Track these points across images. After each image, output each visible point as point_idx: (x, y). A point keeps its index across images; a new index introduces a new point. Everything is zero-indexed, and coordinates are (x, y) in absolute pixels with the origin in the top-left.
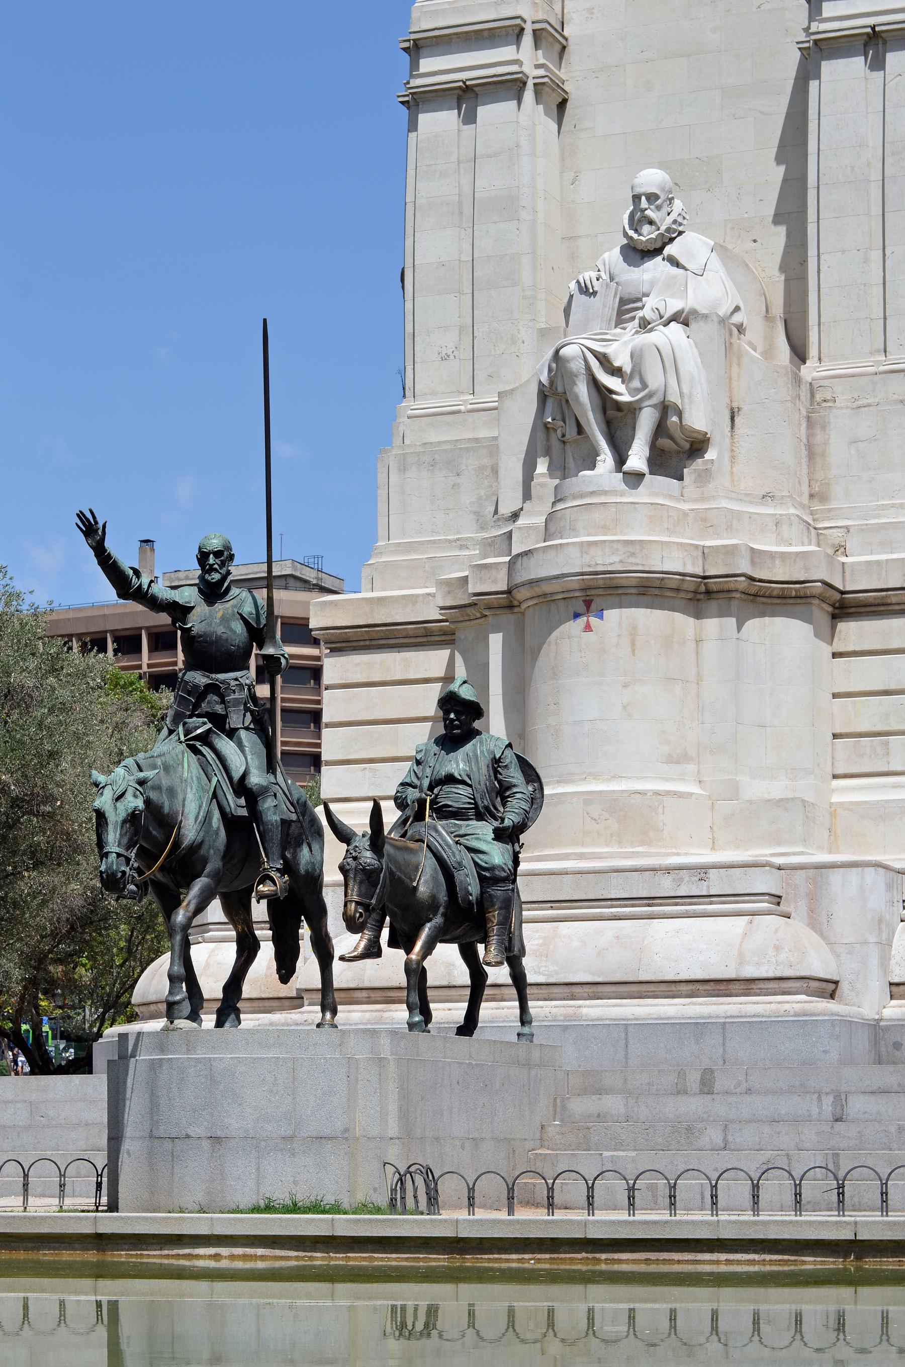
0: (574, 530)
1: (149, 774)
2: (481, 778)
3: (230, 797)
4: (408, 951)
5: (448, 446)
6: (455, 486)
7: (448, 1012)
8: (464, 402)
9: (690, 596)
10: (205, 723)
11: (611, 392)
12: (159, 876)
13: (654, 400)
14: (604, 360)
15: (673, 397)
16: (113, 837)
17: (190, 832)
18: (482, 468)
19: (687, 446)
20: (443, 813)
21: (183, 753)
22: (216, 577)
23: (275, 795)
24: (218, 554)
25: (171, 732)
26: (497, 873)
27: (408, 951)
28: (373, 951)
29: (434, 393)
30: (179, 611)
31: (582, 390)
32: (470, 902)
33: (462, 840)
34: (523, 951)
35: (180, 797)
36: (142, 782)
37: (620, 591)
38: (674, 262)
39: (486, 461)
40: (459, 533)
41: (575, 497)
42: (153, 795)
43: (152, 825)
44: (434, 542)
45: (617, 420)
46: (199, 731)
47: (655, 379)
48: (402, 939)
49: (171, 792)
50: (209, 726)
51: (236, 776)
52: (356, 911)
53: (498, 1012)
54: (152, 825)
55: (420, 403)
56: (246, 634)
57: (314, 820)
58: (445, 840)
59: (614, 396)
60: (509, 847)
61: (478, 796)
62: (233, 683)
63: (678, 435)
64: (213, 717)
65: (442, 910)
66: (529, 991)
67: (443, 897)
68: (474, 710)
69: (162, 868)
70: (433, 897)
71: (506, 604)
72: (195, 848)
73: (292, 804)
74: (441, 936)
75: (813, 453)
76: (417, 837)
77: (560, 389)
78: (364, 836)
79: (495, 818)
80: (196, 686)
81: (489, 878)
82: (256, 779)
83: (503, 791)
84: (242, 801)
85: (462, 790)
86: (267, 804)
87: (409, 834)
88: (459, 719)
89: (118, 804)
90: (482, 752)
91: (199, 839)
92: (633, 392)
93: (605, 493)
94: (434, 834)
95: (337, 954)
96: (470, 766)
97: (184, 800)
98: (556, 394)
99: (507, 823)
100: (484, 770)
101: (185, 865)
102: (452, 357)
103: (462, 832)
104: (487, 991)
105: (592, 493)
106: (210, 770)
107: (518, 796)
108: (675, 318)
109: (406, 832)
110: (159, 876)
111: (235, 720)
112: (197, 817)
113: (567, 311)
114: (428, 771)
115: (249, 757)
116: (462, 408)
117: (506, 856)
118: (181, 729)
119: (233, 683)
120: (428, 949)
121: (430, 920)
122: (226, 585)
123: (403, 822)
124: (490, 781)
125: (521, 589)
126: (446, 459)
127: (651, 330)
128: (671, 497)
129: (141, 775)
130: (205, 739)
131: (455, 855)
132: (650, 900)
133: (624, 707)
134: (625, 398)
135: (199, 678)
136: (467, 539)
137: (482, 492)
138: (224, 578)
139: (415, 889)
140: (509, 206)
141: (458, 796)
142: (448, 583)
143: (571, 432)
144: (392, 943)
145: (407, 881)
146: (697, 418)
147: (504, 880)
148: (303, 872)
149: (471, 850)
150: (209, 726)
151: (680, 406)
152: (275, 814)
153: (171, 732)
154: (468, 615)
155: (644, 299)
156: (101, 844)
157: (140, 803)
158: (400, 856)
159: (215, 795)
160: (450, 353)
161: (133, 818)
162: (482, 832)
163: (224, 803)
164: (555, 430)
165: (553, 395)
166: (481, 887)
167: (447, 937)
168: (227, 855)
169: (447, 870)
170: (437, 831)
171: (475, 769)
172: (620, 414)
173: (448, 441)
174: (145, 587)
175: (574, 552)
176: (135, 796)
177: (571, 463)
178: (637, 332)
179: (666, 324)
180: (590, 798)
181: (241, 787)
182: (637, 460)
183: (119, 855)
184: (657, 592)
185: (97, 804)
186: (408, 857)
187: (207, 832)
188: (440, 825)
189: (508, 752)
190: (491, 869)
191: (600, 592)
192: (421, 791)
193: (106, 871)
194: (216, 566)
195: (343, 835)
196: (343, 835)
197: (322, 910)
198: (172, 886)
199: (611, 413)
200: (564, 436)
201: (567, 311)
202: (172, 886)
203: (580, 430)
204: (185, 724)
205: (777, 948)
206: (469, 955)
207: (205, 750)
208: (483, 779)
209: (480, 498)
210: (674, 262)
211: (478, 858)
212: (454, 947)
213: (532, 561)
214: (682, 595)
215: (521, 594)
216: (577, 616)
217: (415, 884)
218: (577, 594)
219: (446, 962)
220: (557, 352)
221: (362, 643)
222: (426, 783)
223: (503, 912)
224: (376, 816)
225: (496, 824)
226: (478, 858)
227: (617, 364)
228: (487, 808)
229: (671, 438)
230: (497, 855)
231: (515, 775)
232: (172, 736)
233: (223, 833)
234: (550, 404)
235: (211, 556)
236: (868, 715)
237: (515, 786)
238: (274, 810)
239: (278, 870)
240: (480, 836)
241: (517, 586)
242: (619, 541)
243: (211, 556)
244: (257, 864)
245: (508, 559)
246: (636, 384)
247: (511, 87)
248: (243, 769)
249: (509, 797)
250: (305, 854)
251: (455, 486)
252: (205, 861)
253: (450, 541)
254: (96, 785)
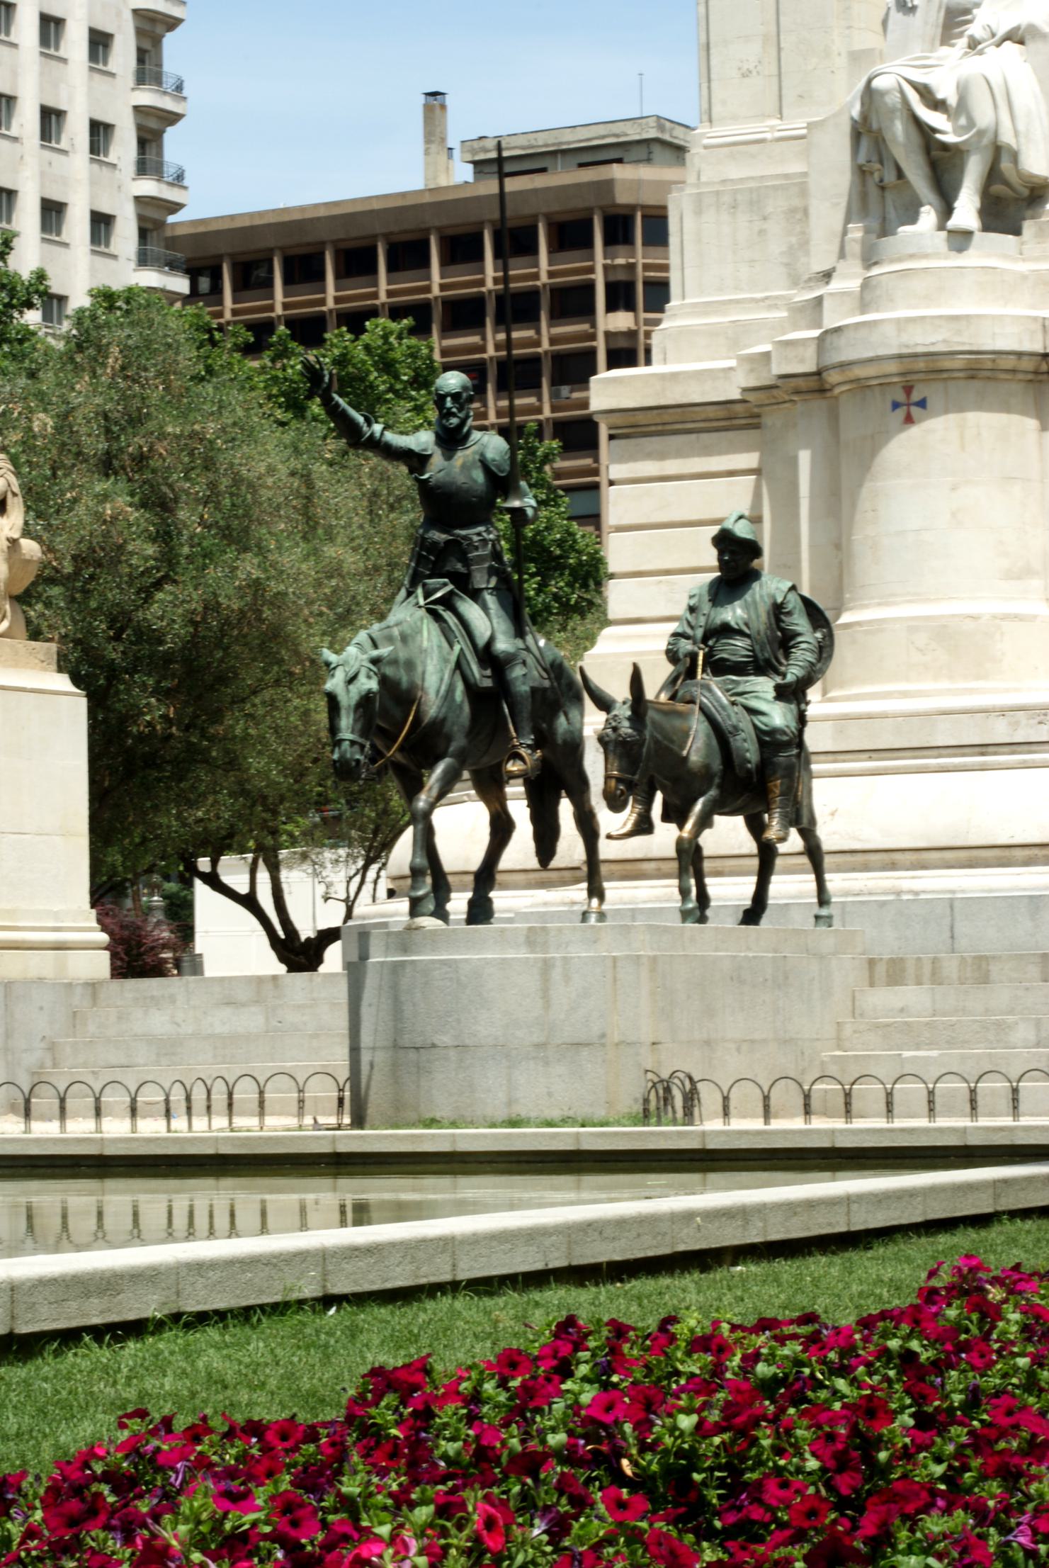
0: (892, 300)
1: (384, 651)
2: (762, 628)
3: (475, 668)
4: (681, 827)
5: (752, 184)
6: (762, 232)
7: (731, 891)
8: (769, 127)
9: (1030, 377)
10: (445, 585)
11: (935, 130)
12: (400, 758)
13: (986, 141)
14: (925, 92)
15: (1007, 137)
16: (346, 721)
17: (432, 707)
18: (793, 211)
19: (1026, 192)
20: (719, 667)
21: (422, 619)
22: (454, 421)
23: (524, 663)
24: (456, 396)
25: (409, 594)
26: (779, 737)
27: (681, 827)
28: (643, 826)
29: (735, 118)
30: (416, 461)
31: (898, 130)
32: (749, 771)
33: (739, 699)
34: (813, 821)
35: (420, 669)
36: (375, 661)
37: (945, 375)
39: (796, 202)
40: (766, 289)
41: (892, 261)
42: (389, 671)
43: (391, 702)
44: (737, 302)
45: (942, 165)
46: (439, 595)
47: (984, 116)
48: (675, 814)
49: (410, 665)
50: (450, 587)
51: (481, 642)
52: (617, 788)
53: (791, 885)
54: (391, 702)
55: (718, 130)
56: (484, 488)
57: (571, 684)
58: (718, 700)
59: (938, 136)
60: (793, 706)
61: (757, 648)
62: (476, 538)
63: (1013, 179)
65: (717, 781)
66: (828, 861)
67: (717, 765)
68: (752, 549)
69: (401, 749)
70: (707, 767)
71: (814, 386)
72: (438, 726)
73: (545, 670)
74: (722, 806)
76: (688, 698)
77: (875, 126)
78: (624, 703)
79: (778, 673)
80: (435, 543)
81: (770, 741)
82: (504, 644)
83: (786, 641)
84: (488, 672)
85: (740, 643)
86: (517, 672)
87: (680, 694)
88: (737, 560)
89: (351, 687)
90: (761, 597)
91: (441, 715)
92: (958, 130)
93: (926, 256)
94: (707, 694)
95: (603, 832)
96: (748, 613)
97: (424, 673)
98: (870, 131)
99: (790, 678)
100: (764, 617)
101: (425, 744)
102: (754, 73)
103: (740, 689)
104: (779, 862)
105: (912, 257)
106: (452, 637)
107: (803, 646)
108: (1008, 37)
109: (677, 692)
110: (400, 758)
111: (480, 579)
112: (438, 691)
113: (885, 23)
114: (702, 621)
115: (495, 621)
116: (768, 136)
117: (789, 717)
118: (420, 591)
119: (476, 538)
120: (705, 822)
121: (702, 795)
122: (466, 429)
123: (673, 681)
124: (772, 630)
125: (831, 372)
126: (751, 199)
127: (981, 53)
128: (1006, 257)
129: (375, 653)
130: (447, 602)
131: (734, 717)
132: (983, 748)
133: (954, 515)
134: (949, 137)
135: (438, 536)
136: (777, 297)
137: (794, 240)
138: (463, 422)
139: (686, 759)
141: (738, 648)
142: (751, 359)
143: (890, 177)
144: (666, 817)
145: (675, 748)
147: (787, 745)
148: (560, 741)
149: (752, 712)
150: (450, 587)
151: (1015, 146)
152: (524, 683)
153: (409, 594)
154: (774, 397)
155: (975, 11)
156: (333, 729)
157: (373, 685)
158: (667, 723)
159: (458, 666)
160: (751, 68)
161: (366, 701)
162: (764, 686)
163: (468, 672)
164: (872, 173)
165: (866, 133)
166: (762, 753)
167: (726, 810)
168: (473, 730)
169: (721, 735)
170: (710, 690)
171: (754, 617)
172: (947, 154)
173: (752, 178)
174: (378, 435)
176: (369, 677)
177: (892, 214)
178: (966, 53)
179: (998, 45)
180: (914, 626)
181: (487, 655)
182: (967, 210)
183: (353, 743)
184: (988, 374)
185: (329, 686)
186: (677, 723)
187: (449, 708)
188: (715, 683)
189: (792, 597)
190: (773, 732)
191: (921, 376)
192: (695, 643)
193: (339, 761)
194: (454, 410)
195: (604, 703)
196: (604, 703)
197: (583, 782)
198: (413, 768)
199: (935, 153)
200: (881, 181)
201: (885, 23)
202: (413, 768)
203: (900, 174)
204: (424, 585)
206: (756, 827)
207: (448, 616)
208: (762, 628)
209: (791, 247)
211: (758, 721)
212: (739, 821)
213: (842, 341)
214: (1021, 376)
215: (833, 377)
216: (896, 405)
217: (685, 753)
218: (895, 379)
219: (728, 834)
220: (869, 81)
221: (653, 428)
222: (699, 633)
223: (786, 780)
224: (636, 681)
225: (779, 680)
226: (758, 721)
227: (940, 96)
228: (768, 661)
229: (1007, 183)
230: (779, 716)
231: (799, 622)
232: (411, 599)
233: (467, 708)
234: (865, 143)
235: (449, 399)
237: (799, 634)
238: (523, 678)
239: (529, 746)
240: (761, 695)
241: (827, 369)
242: (940, 317)
243: (449, 399)
244: (512, 732)
245: (816, 333)
246: (963, 121)
248: (488, 634)
249: (793, 647)
250: (562, 722)
251: (762, 232)
252: (449, 739)
253: (756, 301)
254: (328, 664)
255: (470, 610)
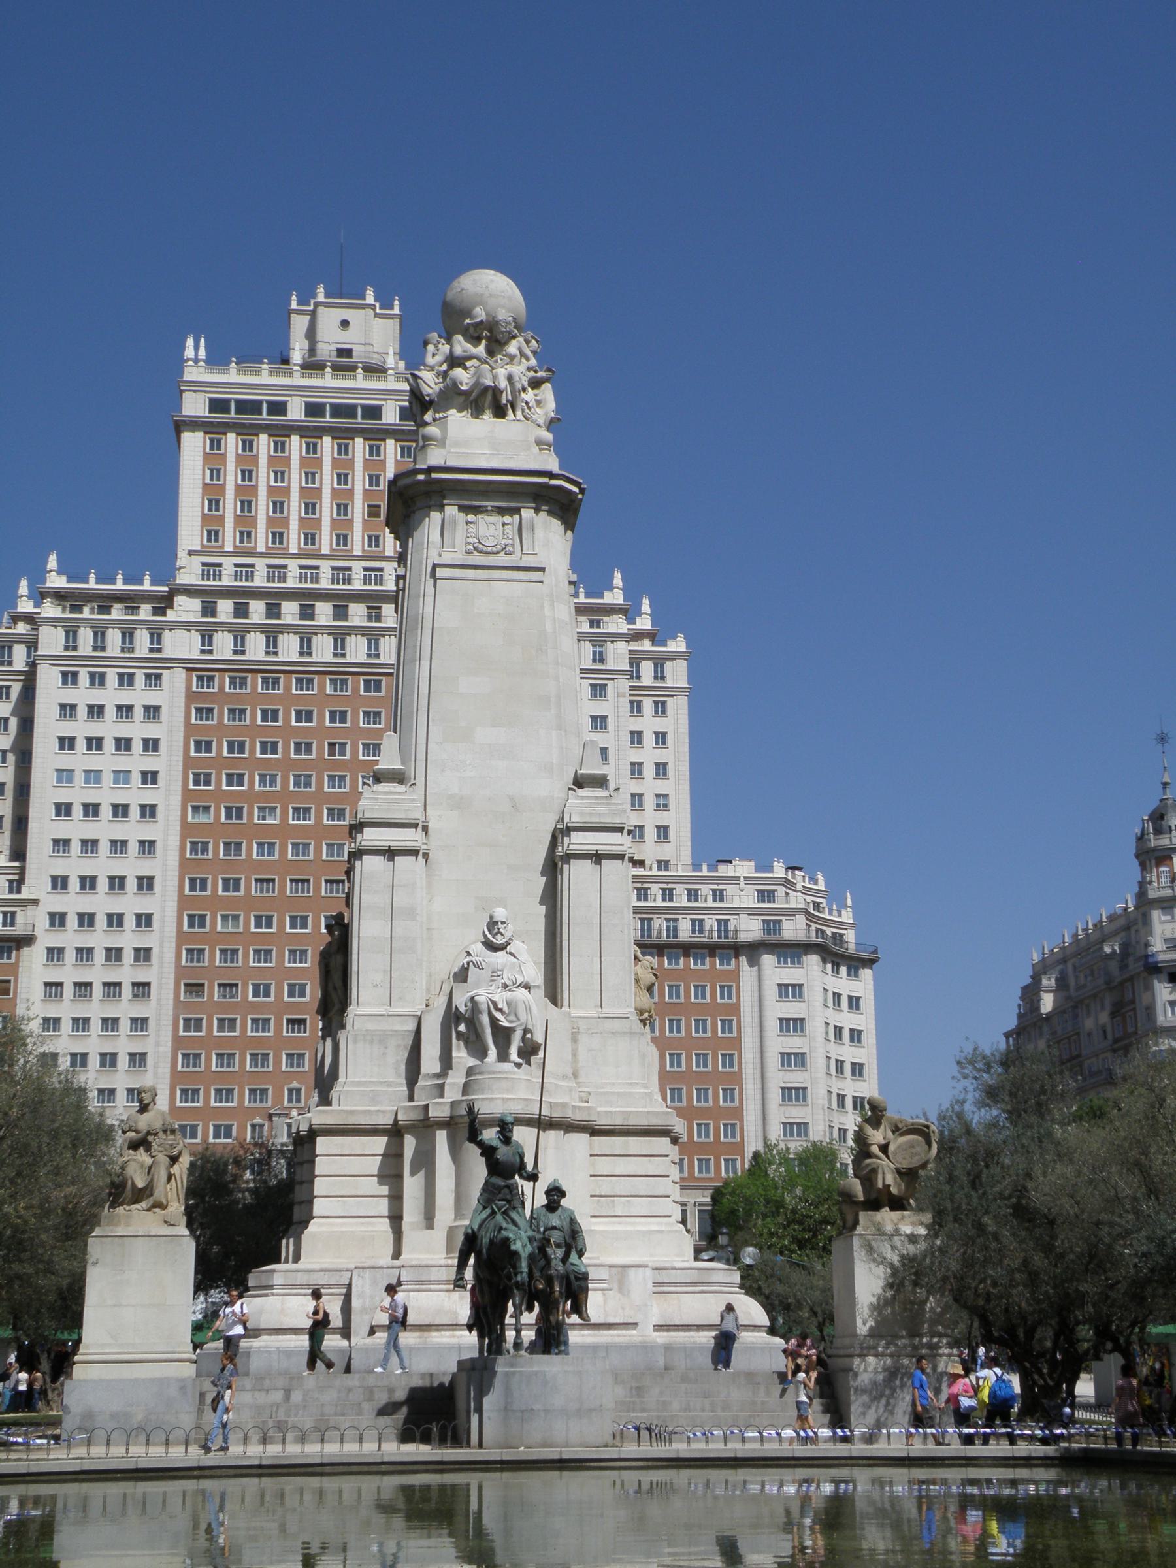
6: (384, 1054)
8: (383, 1010)
14: (495, 1004)
31: (485, 1019)
38: (512, 954)
41: (490, 1073)
45: (502, 1035)
47: (523, 1016)
64: (509, 1202)
75: (574, 1055)
134: (506, 1024)
135: (500, 1182)
140: (411, 913)
146: (539, 1038)
175: (500, 1102)
205: (623, 1308)
210: (512, 954)
236: (605, 1186)
247: (414, 852)
251: (384, 1054)
255: (514, 1215)
